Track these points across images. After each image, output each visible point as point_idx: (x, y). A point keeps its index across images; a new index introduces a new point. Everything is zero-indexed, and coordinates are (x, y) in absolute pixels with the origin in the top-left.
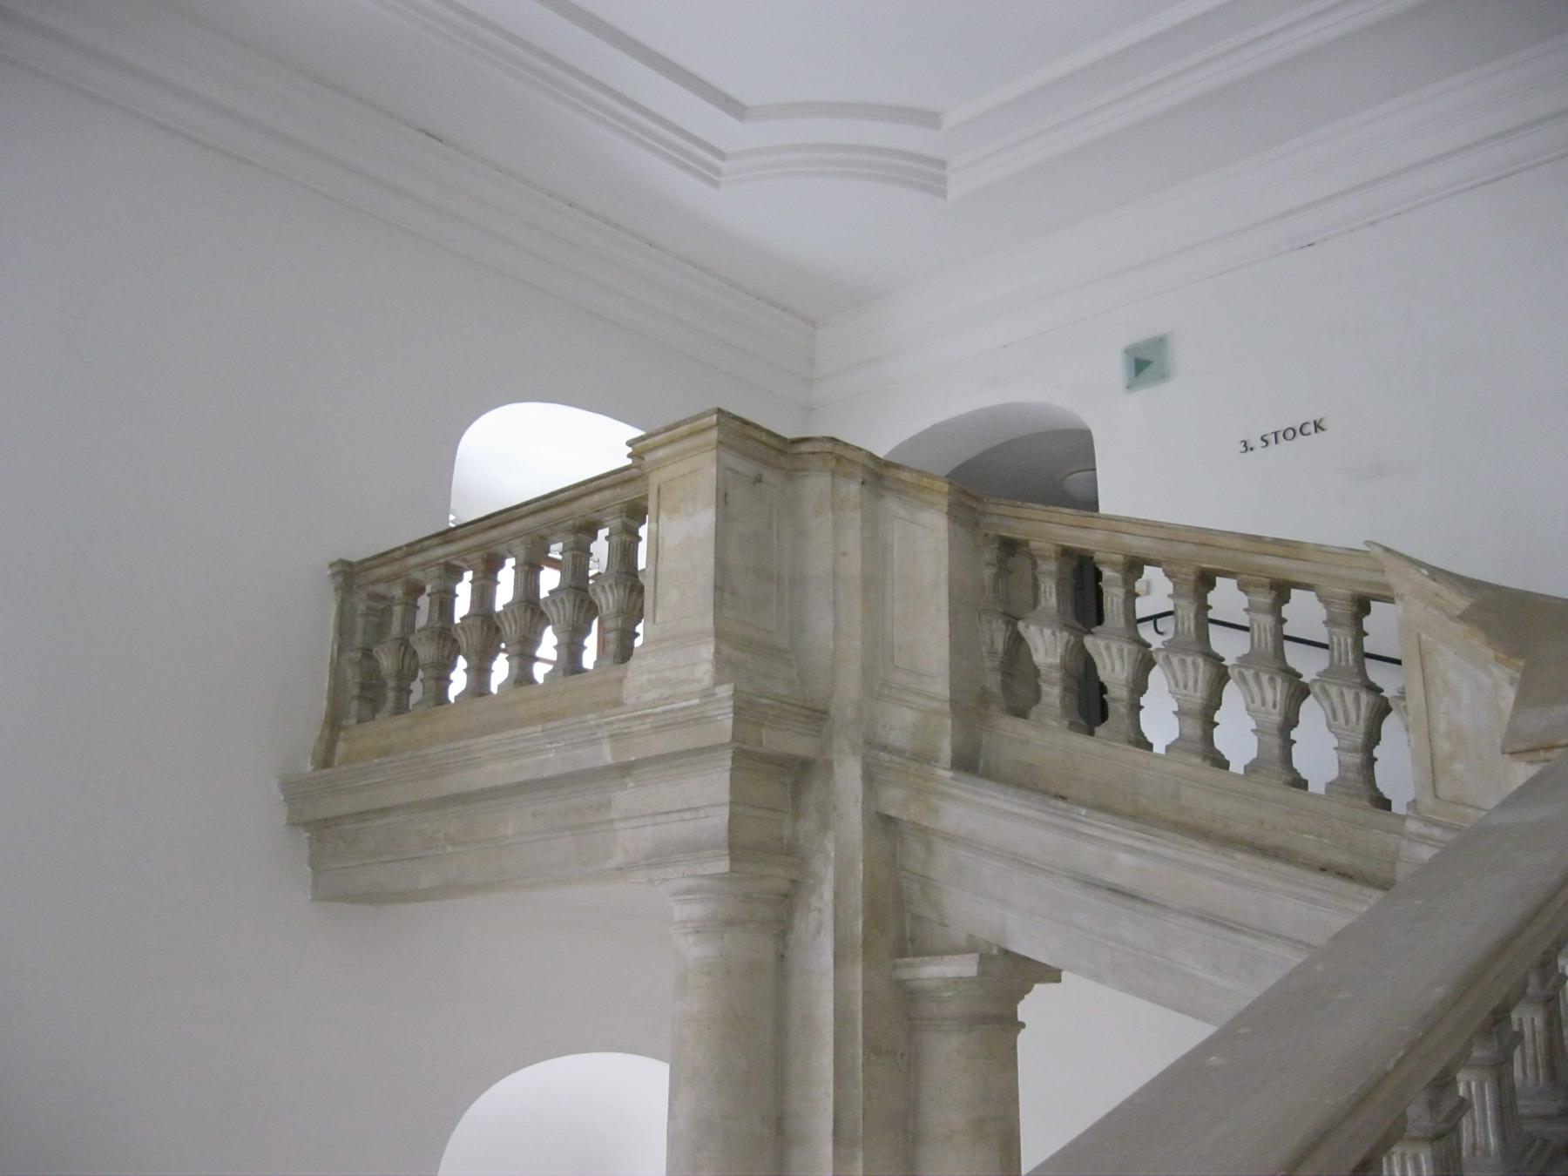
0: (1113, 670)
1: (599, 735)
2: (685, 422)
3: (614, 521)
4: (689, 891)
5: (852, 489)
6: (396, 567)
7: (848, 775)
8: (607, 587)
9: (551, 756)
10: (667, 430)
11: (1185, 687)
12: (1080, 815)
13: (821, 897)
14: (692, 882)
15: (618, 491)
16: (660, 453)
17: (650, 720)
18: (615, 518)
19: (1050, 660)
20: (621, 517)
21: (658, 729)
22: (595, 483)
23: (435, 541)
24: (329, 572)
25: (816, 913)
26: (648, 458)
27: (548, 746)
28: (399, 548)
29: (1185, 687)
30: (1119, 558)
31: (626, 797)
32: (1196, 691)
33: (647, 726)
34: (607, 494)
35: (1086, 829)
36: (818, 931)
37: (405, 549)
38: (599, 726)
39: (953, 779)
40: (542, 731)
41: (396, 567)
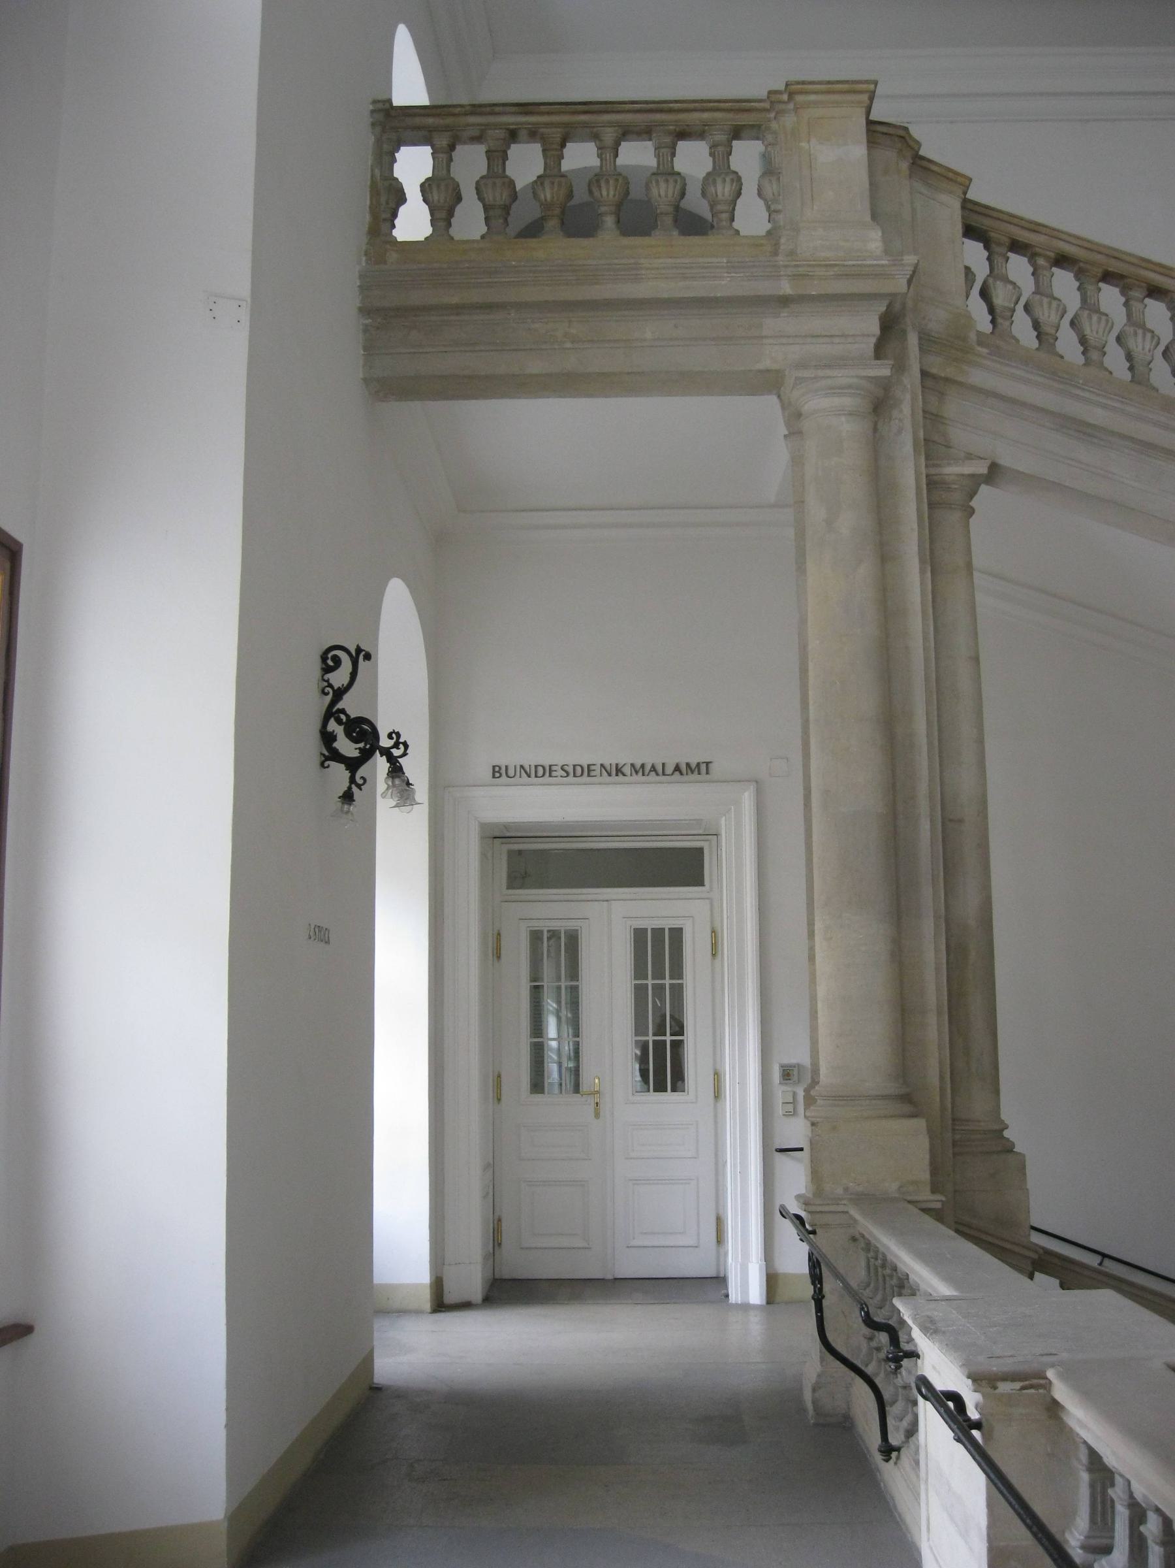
0: (1049, 316)
1: (782, 273)
2: (847, 82)
3: (723, 136)
4: (850, 387)
5: (904, 166)
6: (449, 121)
7: (913, 340)
8: (728, 179)
9: (723, 283)
10: (829, 82)
11: (1097, 332)
12: (1079, 383)
13: (901, 411)
14: (855, 380)
15: (730, 115)
16: (813, 97)
17: (836, 269)
18: (724, 134)
19: (1006, 304)
20: (730, 134)
21: (838, 277)
22: (671, 105)
23: (513, 109)
24: (371, 107)
25: (897, 421)
26: (800, 98)
27: (726, 275)
28: (461, 106)
29: (1097, 332)
30: (1052, 255)
31: (772, 324)
32: (1103, 336)
33: (832, 273)
34: (718, 115)
35: (1078, 392)
36: (900, 431)
37: (468, 108)
38: (786, 266)
39: (988, 354)
40: (727, 263)
41: (449, 121)
